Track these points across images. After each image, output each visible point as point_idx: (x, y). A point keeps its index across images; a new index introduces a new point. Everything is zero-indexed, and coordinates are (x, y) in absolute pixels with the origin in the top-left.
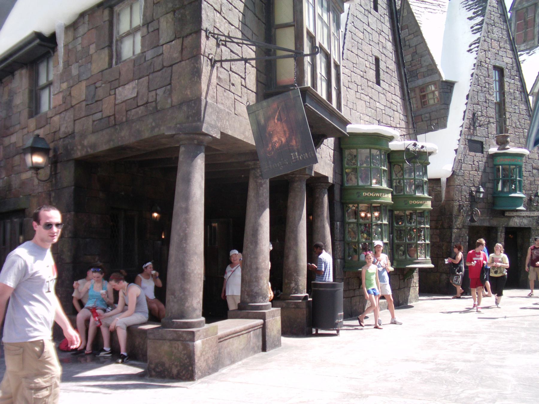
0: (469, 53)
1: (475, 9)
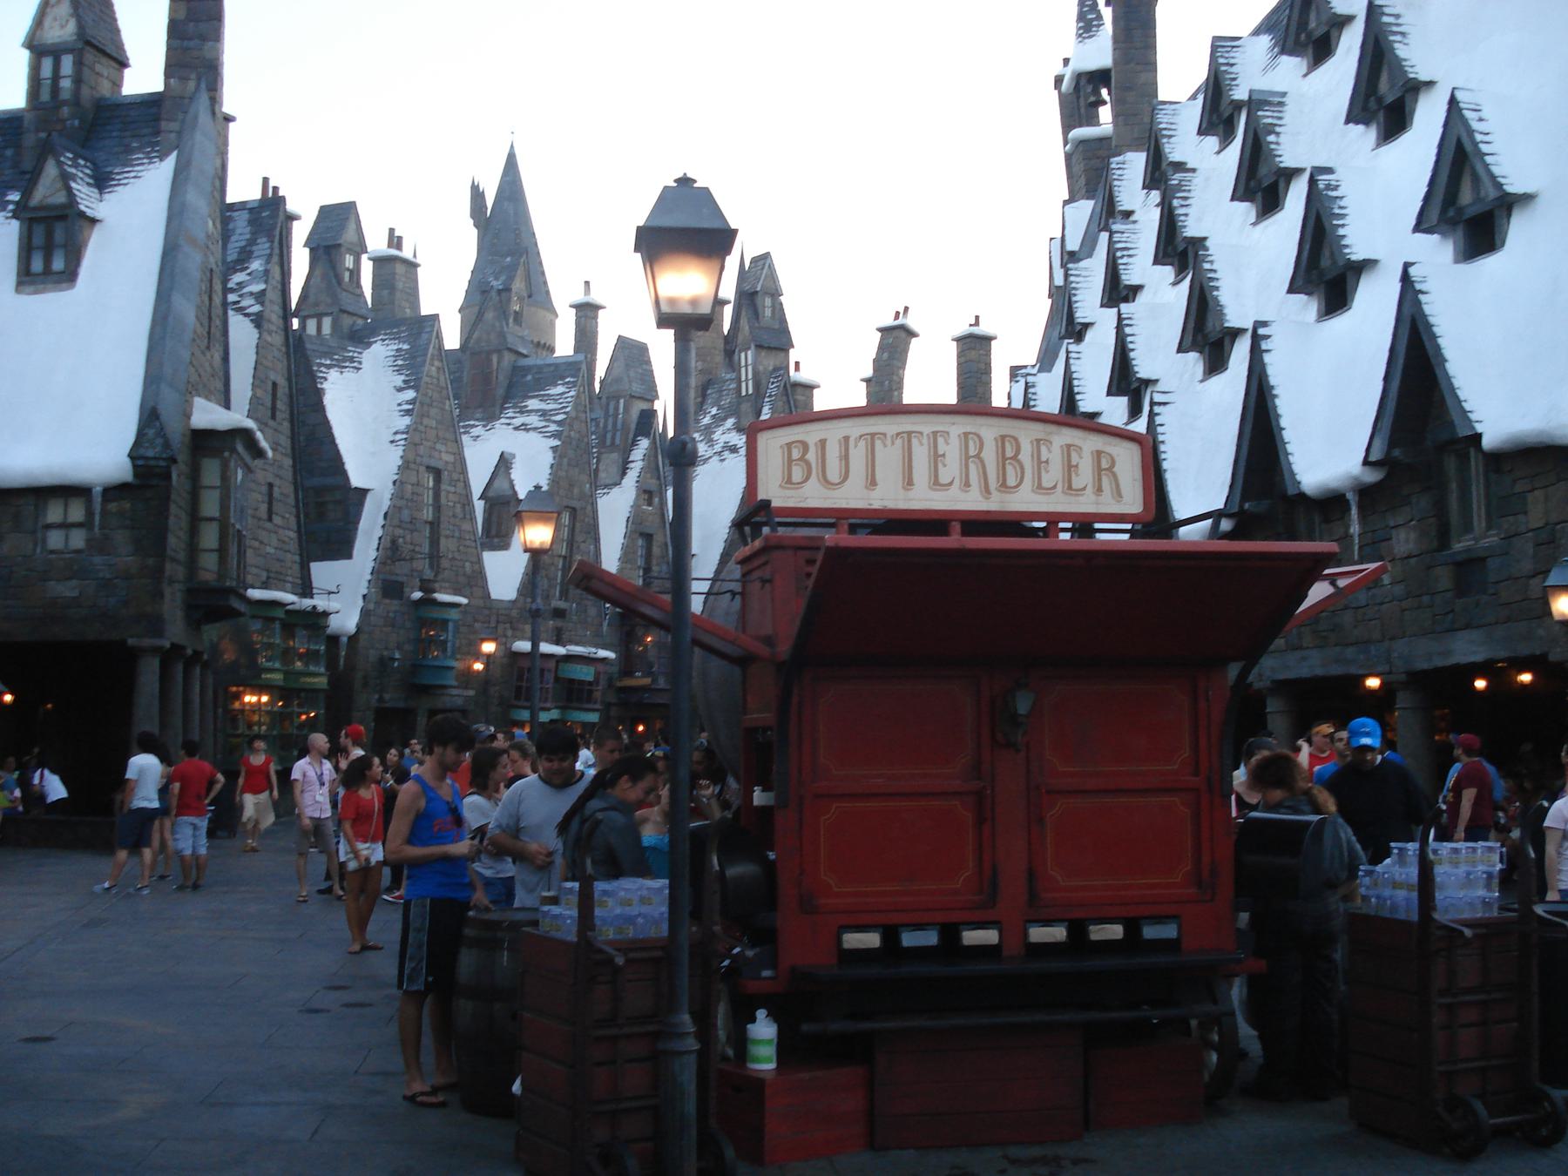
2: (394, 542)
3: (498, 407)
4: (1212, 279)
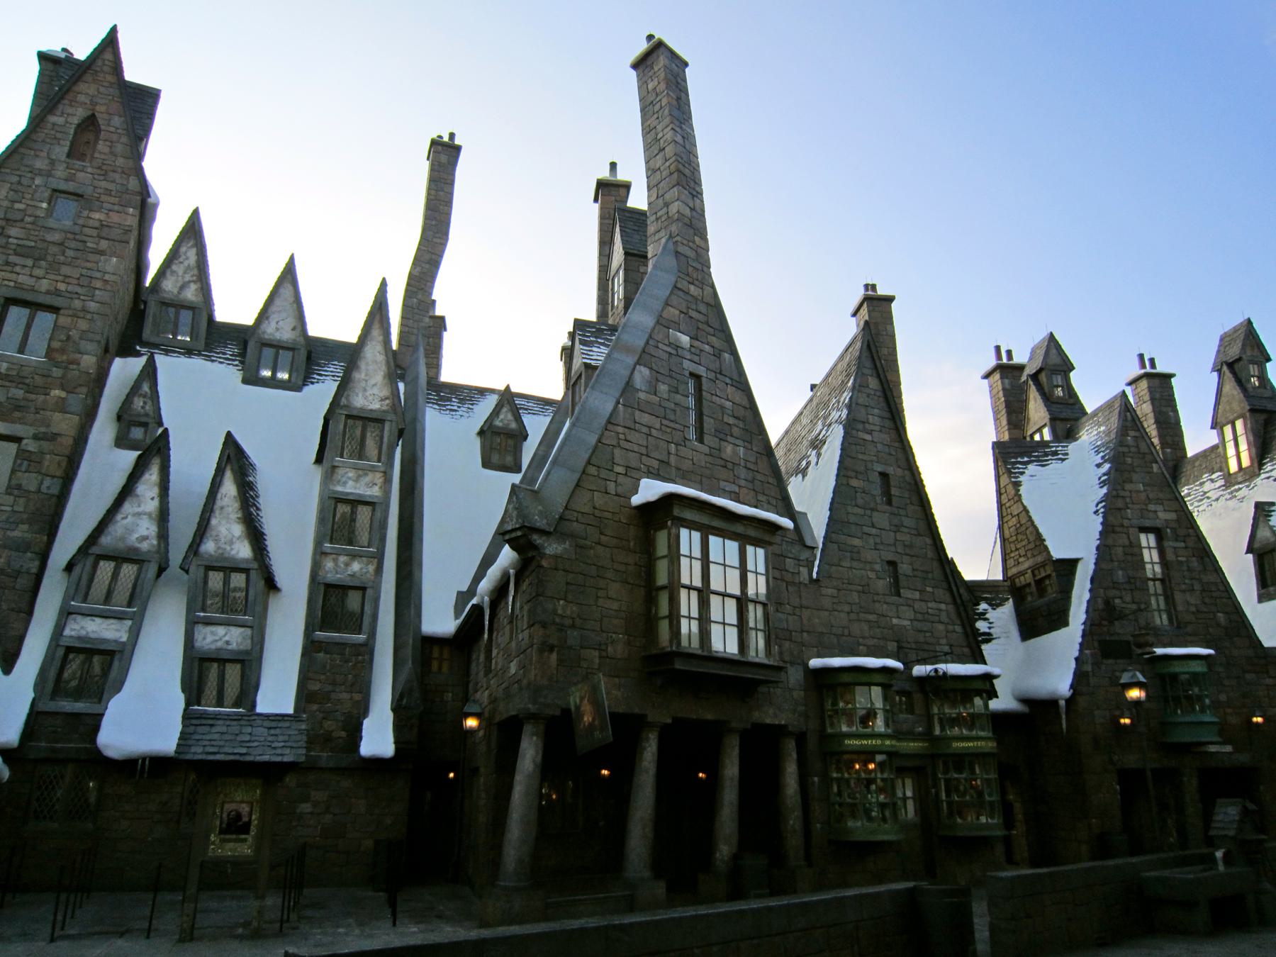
0: (1095, 516)
1: (1103, 452)
2: (1107, 603)
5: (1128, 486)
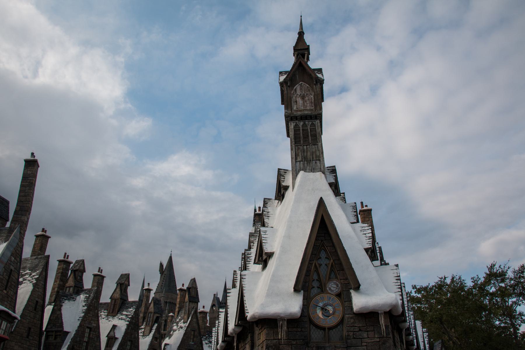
2: (73, 346)
3: (116, 313)
4: (235, 279)
5: (89, 315)
